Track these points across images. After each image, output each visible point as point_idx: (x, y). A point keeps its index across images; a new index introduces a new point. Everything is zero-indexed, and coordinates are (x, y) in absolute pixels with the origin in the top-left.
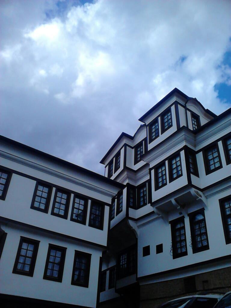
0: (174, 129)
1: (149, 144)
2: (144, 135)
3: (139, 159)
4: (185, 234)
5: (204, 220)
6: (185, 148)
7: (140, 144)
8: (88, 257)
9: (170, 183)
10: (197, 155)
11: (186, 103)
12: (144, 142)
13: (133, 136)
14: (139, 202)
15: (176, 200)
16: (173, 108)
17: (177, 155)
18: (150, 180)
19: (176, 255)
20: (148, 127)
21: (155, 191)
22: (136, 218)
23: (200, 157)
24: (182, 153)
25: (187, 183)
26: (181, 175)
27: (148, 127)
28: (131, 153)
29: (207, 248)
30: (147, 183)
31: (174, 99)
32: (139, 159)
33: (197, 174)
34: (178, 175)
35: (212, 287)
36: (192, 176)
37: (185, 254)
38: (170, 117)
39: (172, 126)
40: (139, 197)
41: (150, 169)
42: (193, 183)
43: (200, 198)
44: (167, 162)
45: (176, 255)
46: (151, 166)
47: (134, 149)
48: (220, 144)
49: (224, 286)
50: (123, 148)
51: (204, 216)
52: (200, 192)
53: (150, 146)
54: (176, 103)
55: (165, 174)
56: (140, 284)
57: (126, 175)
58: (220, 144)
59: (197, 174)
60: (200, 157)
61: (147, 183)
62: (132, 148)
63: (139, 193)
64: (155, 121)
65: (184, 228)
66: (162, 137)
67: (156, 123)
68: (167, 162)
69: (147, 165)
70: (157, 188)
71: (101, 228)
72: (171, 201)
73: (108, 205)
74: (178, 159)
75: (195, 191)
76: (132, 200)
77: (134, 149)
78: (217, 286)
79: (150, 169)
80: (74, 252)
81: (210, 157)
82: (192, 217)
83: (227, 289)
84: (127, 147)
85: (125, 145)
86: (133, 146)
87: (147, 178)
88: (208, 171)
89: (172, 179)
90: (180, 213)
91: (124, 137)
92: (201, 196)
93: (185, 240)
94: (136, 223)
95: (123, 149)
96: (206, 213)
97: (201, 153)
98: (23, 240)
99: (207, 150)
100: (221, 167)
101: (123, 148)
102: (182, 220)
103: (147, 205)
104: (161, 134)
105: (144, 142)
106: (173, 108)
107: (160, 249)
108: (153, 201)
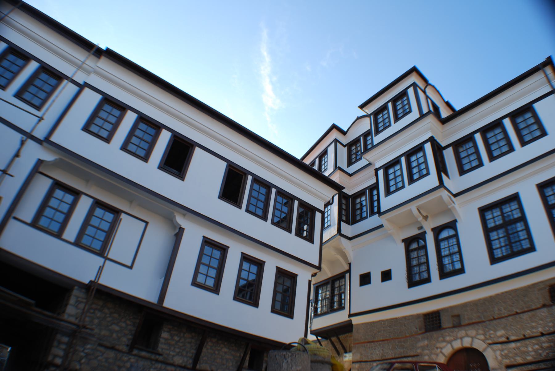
0: (415, 114)
1: (375, 136)
2: (366, 125)
3: (353, 160)
4: (426, 255)
5: (456, 236)
6: (432, 140)
7: (356, 142)
8: (293, 277)
9: (409, 184)
10: (445, 152)
11: (426, 87)
12: (362, 138)
13: (345, 130)
14: (354, 215)
15: (418, 209)
16: (411, 91)
17: (419, 148)
18: (377, 184)
19: (412, 283)
20: (372, 116)
21: (386, 196)
22: (350, 236)
23: (449, 155)
24: (428, 147)
25: (437, 183)
26: (428, 174)
27: (372, 116)
28: (343, 152)
29: (461, 271)
30: (367, 191)
31: (413, 78)
32: (353, 160)
33: (447, 175)
34: (422, 175)
35: (467, 322)
36: (444, 176)
37: (428, 280)
38: (406, 102)
39: (410, 111)
40: (354, 210)
42: (445, 184)
43: (453, 204)
44: (403, 159)
45: (412, 283)
46: (378, 165)
47: (347, 147)
48: (478, 137)
49: (484, 320)
50: (333, 143)
51: (455, 229)
52: (452, 197)
53: (377, 139)
54: (414, 85)
55: (402, 175)
56: (353, 323)
57: (338, 179)
58: (478, 137)
59: (447, 175)
60: (449, 155)
61: (367, 191)
62: (344, 146)
63: (354, 204)
64: (384, 107)
65: (425, 247)
66: (395, 127)
67: (383, 112)
68: (403, 159)
69: (370, 164)
70: (388, 192)
71: (310, 239)
72: (411, 210)
73: (320, 211)
74: (420, 154)
75: (448, 195)
76: (344, 213)
77: (347, 147)
78: (474, 321)
79: (377, 170)
80: (275, 269)
81: (463, 155)
82: (437, 231)
83: (488, 323)
84: (338, 144)
85: (336, 141)
86: (345, 144)
87: (374, 181)
88: (462, 172)
89: (411, 180)
90: (418, 228)
91: (334, 130)
92: (453, 202)
93: (427, 262)
95: (332, 146)
96: (458, 225)
97: (450, 149)
98: (207, 242)
99: (457, 145)
100: (481, 164)
101: (333, 144)
102: (422, 236)
103: (367, 218)
104: (395, 123)
105: (362, 138)
106: (411, 91)
107: (386, 276)
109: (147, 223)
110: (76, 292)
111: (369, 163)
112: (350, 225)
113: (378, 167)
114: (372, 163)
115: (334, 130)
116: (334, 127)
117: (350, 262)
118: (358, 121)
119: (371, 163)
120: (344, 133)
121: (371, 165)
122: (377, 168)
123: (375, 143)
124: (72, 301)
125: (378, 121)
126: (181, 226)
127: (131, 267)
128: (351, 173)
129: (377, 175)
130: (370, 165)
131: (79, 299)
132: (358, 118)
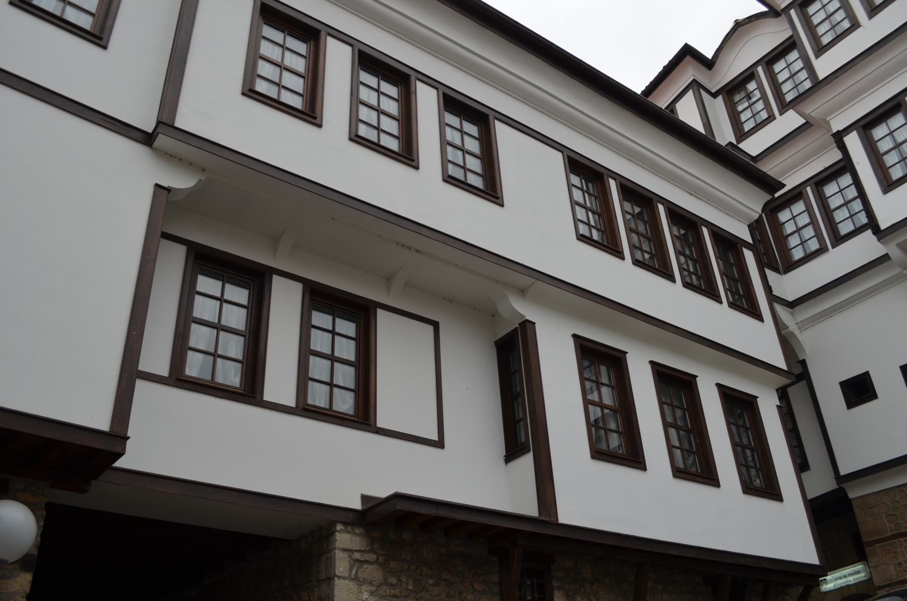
12: (760, 69)
14: (785, 251)
20: (792, 12)
27: (792, 12)
30: (809, 189)
41: (839, 138)
50: (690, 94)
56: (851, 495)
61: (809, 189)
62: (714, 95)
77: (720, 98)
85: (695, 85)
91: (688, 58)
94: (792, 314)
108: (883, 225)
109: (436, 325)
110: (344, 539)
111: (805, 121)
112: (780, 273)
113: (840, 129)
114: (812, 123)
115: (688, 58)
116: (687, 52)
117: (801, 359)
118: (740, 29)
119: (809, 121)
120: (708, 64)
121: (812, 127)
122: (838, 131)
123: (822, 74)
124: (341, 564)
125: (811, 22)
126: (525, 317)
127: (439, 444)
128: (754, 155)
129: (843, 148)
130: (809, 128)
131: (357, 556)
132: (738, 25)
